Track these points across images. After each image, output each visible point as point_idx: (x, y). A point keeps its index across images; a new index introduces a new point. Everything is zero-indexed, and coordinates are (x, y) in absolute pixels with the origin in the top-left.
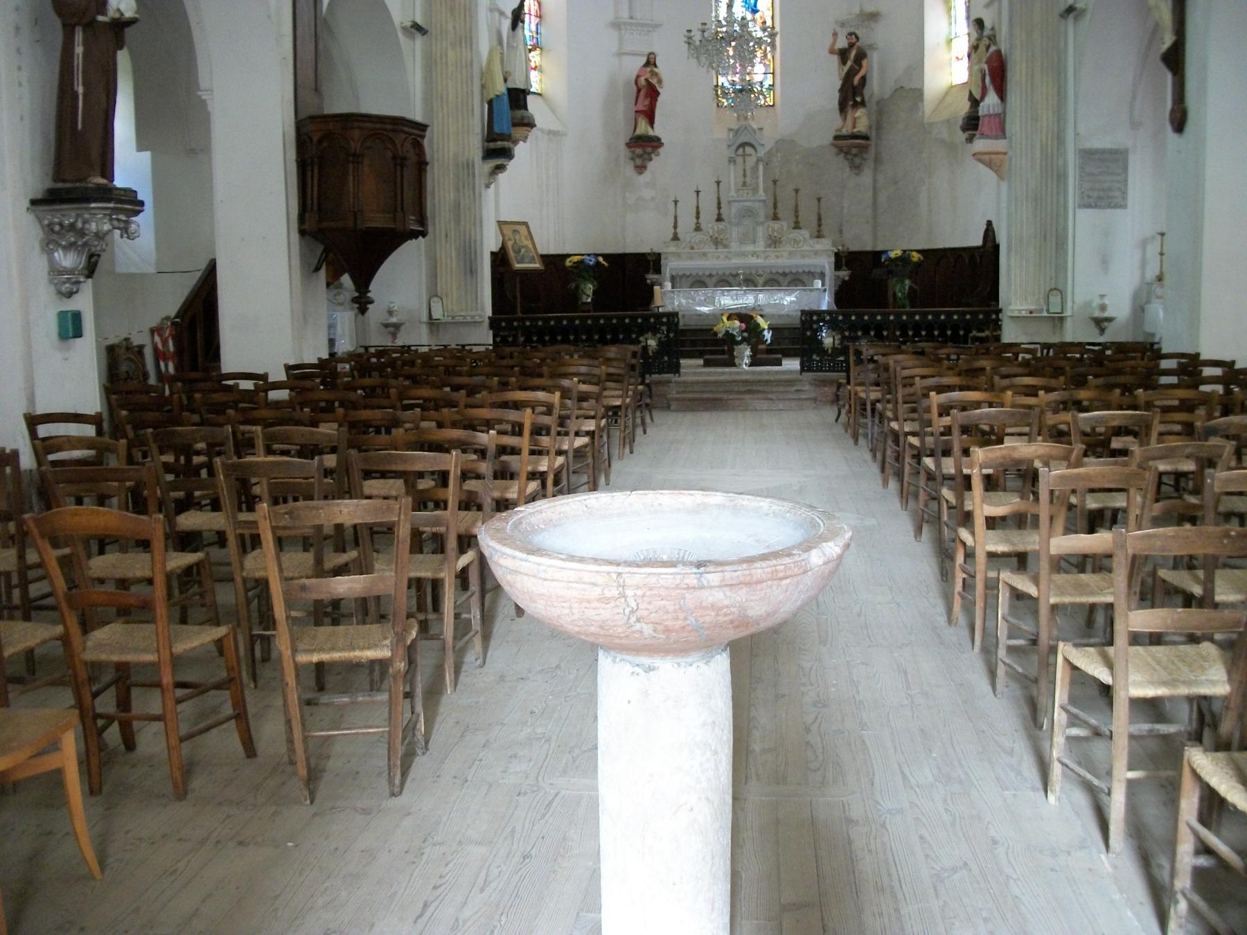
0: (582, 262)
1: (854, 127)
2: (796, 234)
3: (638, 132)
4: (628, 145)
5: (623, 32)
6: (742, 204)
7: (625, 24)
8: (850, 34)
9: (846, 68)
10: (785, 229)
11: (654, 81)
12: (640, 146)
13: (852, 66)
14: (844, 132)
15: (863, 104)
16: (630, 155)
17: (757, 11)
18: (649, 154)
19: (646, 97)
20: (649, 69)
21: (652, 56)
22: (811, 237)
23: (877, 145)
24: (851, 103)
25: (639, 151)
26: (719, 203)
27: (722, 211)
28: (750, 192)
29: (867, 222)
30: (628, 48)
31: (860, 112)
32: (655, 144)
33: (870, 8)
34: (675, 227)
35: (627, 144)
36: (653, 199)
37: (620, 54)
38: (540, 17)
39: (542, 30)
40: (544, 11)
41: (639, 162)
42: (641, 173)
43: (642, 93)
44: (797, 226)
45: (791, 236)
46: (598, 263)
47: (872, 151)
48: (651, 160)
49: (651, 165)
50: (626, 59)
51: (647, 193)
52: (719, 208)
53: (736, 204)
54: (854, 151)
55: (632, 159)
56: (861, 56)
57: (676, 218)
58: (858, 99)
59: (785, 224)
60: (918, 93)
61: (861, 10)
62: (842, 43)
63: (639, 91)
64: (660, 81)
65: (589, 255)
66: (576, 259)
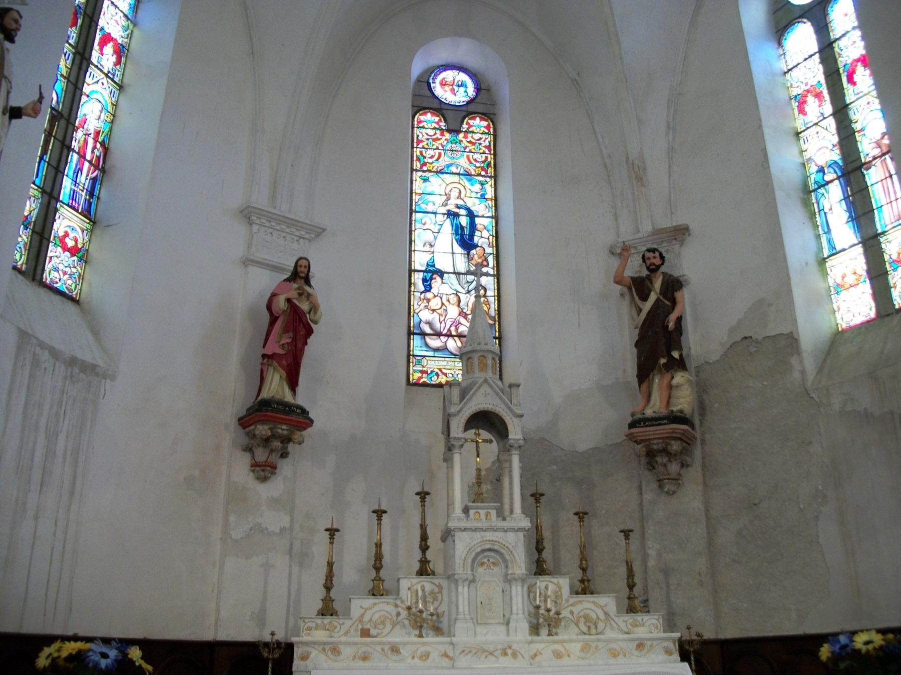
0: (78, 657)
1: (668, 403)
2: (587, 604)
3: (265, 394)
4: (244, 422)
5: (255, 228)
6: (477, 535)
7: (261, 213)
8: (653, 250)
9: (647, 306)
10: (566, 591)
11: (304, 306)
12: (262, 421)
13: (658, 300)
14: (649, 412)
15: (681, 365)
16: (245, 440)
17: (475, 246)
18: (287, 440)
19: (286, 330)
20: (295, 286)
21: (303, 263)
22: (619, 612)
23: (703, 442)
24: (663, 361)
25: (262, 430)
26: (424, 538)
27: (429, 555)
28: (493, 513)
29: (701, 584)
30: (261, 255)
31: (679, 378)
32: (293, 417)
33: (666, 223)
34: (328, 587)
35: (240, 419)
36: (283, 530)
37: (247, 262)
38: (103, 171)
39: (103, 193)
40: (112, 160)
41: (261, 455)
42: (264, 479)
43: (279, 325)
44: (584, 588)
45: (576, 609)
46: (124, 663)
47: (698, 452)
48: (284, 455)
49: (285, 468)
50: (254, 270)
51: (274, 520)
52: (424, 548)
53: (464, 534)
54: (675, 446)
55: (249, 449)
56: (673, 286)
57: (330, 565)
58: (676, 355)
59: (564, 583)
60: (791, 341)
61: (653, 229)
62: (634, 268)
63: (273, 320)
64: (314, 308)
65: (106, 641)
66: (72, 647)
